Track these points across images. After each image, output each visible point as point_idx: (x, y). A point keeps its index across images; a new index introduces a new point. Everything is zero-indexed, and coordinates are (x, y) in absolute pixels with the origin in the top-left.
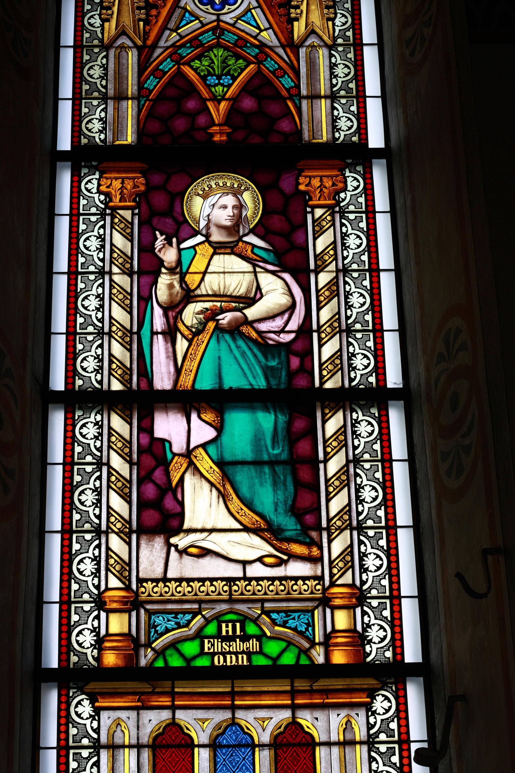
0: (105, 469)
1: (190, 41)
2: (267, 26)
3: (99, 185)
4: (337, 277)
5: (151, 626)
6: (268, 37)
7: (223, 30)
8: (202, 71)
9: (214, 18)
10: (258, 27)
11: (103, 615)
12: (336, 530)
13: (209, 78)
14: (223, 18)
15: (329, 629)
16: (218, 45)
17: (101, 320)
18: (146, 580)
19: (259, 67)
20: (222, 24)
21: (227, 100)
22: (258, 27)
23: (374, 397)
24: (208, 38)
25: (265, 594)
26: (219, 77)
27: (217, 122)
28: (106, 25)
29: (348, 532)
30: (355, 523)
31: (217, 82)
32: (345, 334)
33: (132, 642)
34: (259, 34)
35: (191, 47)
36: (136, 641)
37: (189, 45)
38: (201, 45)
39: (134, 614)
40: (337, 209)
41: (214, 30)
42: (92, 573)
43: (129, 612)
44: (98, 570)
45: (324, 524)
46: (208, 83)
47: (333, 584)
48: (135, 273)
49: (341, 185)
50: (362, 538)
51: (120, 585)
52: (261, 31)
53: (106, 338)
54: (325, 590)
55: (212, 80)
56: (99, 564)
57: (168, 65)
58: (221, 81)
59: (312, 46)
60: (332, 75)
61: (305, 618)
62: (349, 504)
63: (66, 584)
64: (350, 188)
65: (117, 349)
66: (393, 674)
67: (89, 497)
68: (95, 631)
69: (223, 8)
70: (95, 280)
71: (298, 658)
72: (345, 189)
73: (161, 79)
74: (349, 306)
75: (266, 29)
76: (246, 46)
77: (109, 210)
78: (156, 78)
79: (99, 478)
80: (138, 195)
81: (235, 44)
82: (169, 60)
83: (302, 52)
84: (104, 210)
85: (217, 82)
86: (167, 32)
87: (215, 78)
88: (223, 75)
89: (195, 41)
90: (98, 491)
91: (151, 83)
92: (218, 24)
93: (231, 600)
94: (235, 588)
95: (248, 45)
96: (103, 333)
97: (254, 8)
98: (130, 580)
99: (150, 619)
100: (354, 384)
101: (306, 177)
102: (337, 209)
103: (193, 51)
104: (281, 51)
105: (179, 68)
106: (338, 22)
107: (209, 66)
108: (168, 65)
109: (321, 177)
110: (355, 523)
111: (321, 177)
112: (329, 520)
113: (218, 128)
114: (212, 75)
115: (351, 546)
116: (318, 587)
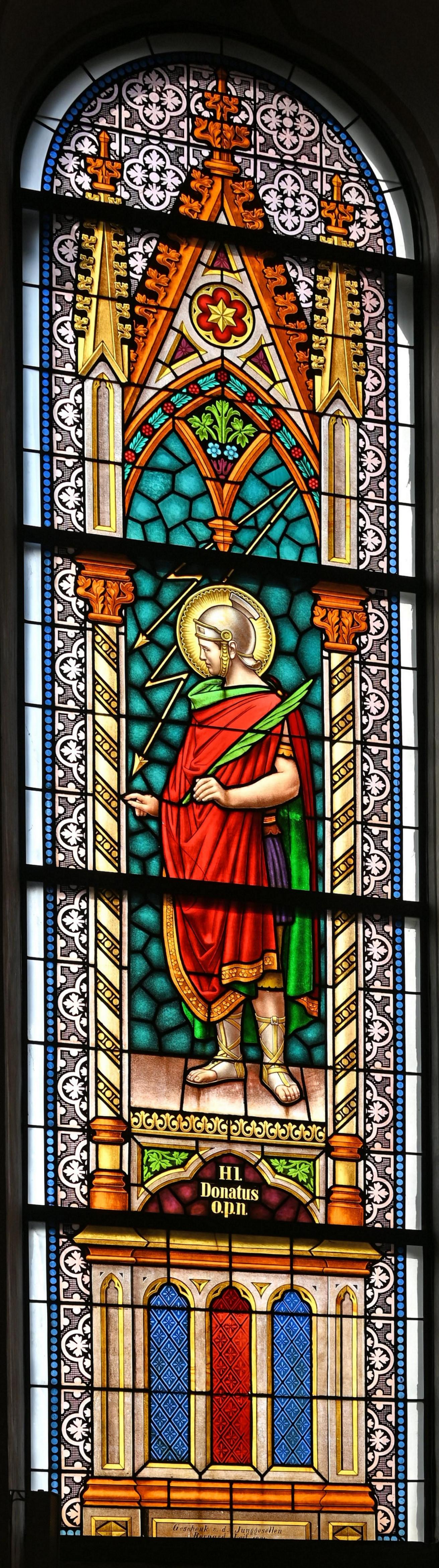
0: (91, 970)
1: (187, 387)
2: (284, 377)
3: (76, 586)
4: (354, 751)
5: (144, 1164)
6: (283, 394)
7: (229, 373)
8: (203, 433)
9: (217, 353)
10: (271, 376)
11: (92, 1146)
12: (342, 1070)
13: (211, 445)
14: (228, 354)
15: (330, 1184)
16: (222, 397)
17: (84, 777)
18: (139, 1110)
19: (271, 438)
20: (226, 363)
21: (232, 483)
22: (271, 376)
23: (387, 911)
24: (209, 384)
25: (266, 1137)
26: (222, 447)
27: (219, 514)
28: (81, 340)
29: (353, 1074)
30: (361, 1065)
31: (219, 452)
32: (359, 827)
33: (123, 1182)
34: (272, 387)
35: (188, 393)
36: (127, 1178)
37: (185, 391)
38: (202, 393)
39: (126, 1147)
40: (357, 658)
41: (216, 371)
42: (80, 1096)
43: (121, 1144)
44: (86, 1093)
45: (330, 1063)
46: (209, 451)
47: (336, 1133)
48: (123, 716)
49: (364, 626)
50: (368, 1082)
51: (110, 1114)
52: (276, 382)
53: (90, 799)
54: (327, 1139)
55: (213, 450)
56: (87, 1084)
57: (158, 419)
58: (226, 453)
59: (336, 416)
60: (361, 467)
61: (305, 1168)
62: (356, 1041)
63: (50, 1107)
64: (373, 631)
65: (104, 818)
66: (392, 1241)
67: (75, 1004)
68: (85, 1165)
69: (228, 339)
70: (76, 721)
71: (297, 1214)
72: (367, 632)
73: (150, 438)
74: (366, 791)
75: (281, 381)
76: (256, 403)
77: (88, 623)
78: (145, 436)
79: (86, 981)
80: (124, 606)
81: (243, 399)
82: (160, 410)
83: (325, 421)
84: (84, 621)
85: (219, 452)
86: (159, 366)
87: (217, 445)
88: (227, 444)
89: (192, 387)
90: (84, 997)
91: (138, 443)
92: (223, 364)
93: (229, 1141)
94: (234, 1127)
95: (260, 402)
96: (87, 794)
97: (267, 345)
98: (121, 1109)
99: (143, 1154)
100: (366, 893)
101: (323, 607)
102: (357, 658)
103: (190, 402)
104: (296, 416)
105: (174, 423)
106: (368, 381)
107: (210, 426)
108: (158, 419)
109: (340, 610)
110: (361, 1065)
111: (340, 610)
112: (335, 1058)
113: (220, 522)
114: (214, 442)
115: (356, 1089)
116: (321, 1134)
